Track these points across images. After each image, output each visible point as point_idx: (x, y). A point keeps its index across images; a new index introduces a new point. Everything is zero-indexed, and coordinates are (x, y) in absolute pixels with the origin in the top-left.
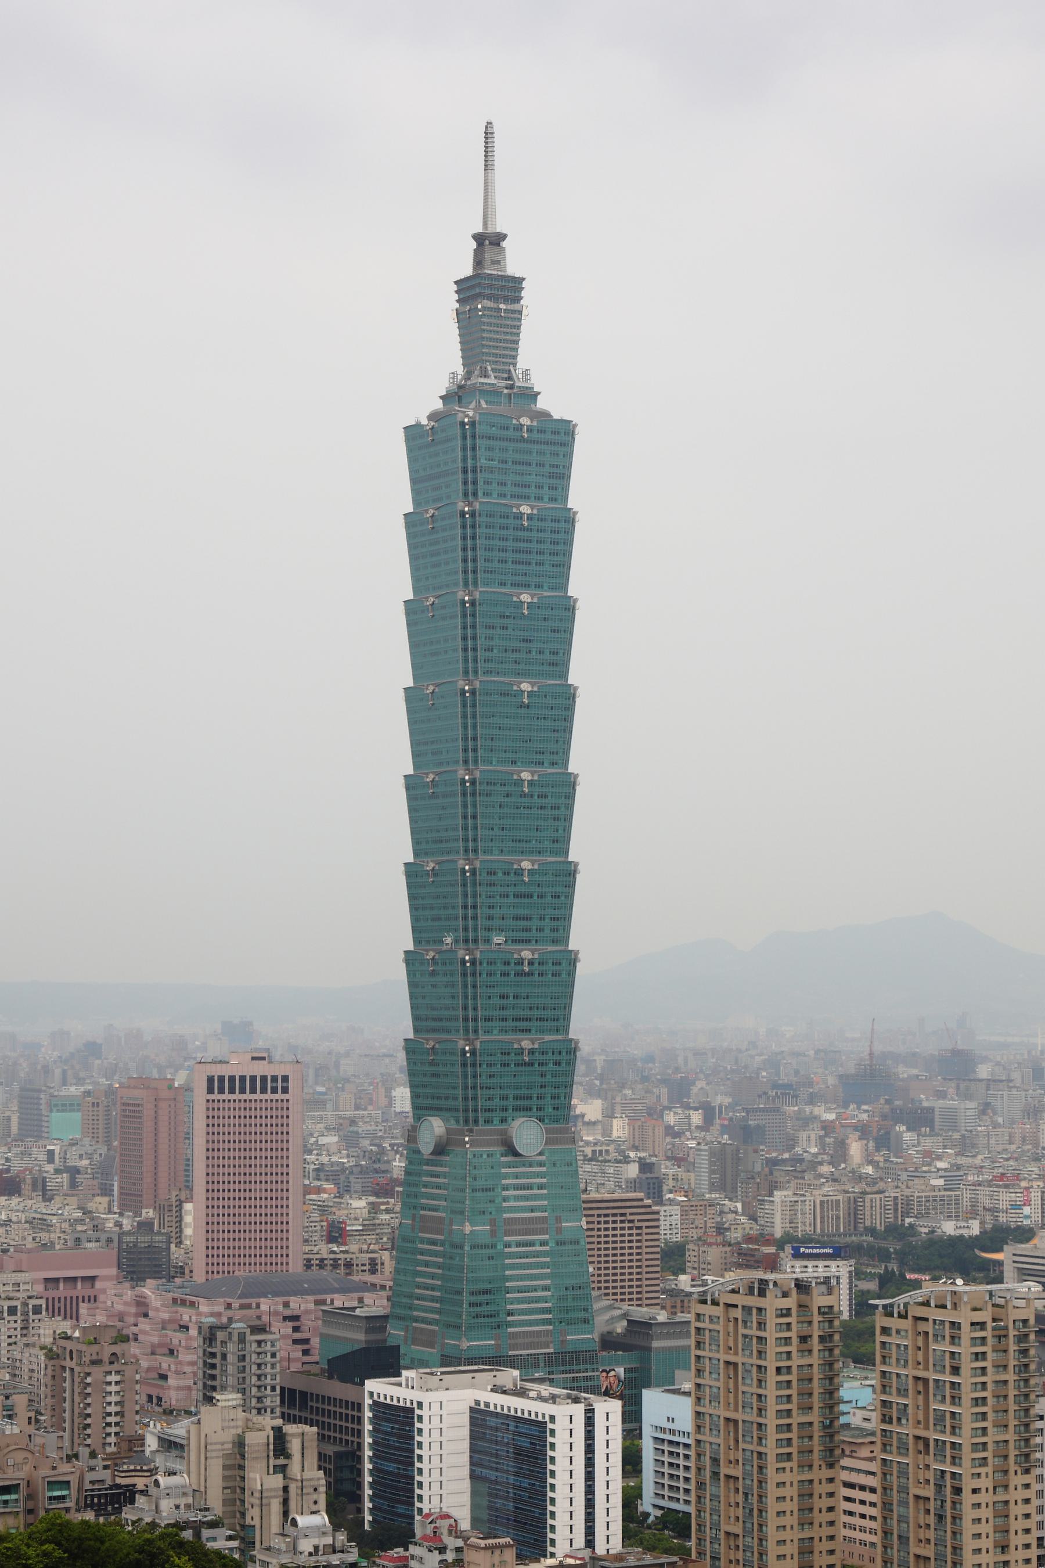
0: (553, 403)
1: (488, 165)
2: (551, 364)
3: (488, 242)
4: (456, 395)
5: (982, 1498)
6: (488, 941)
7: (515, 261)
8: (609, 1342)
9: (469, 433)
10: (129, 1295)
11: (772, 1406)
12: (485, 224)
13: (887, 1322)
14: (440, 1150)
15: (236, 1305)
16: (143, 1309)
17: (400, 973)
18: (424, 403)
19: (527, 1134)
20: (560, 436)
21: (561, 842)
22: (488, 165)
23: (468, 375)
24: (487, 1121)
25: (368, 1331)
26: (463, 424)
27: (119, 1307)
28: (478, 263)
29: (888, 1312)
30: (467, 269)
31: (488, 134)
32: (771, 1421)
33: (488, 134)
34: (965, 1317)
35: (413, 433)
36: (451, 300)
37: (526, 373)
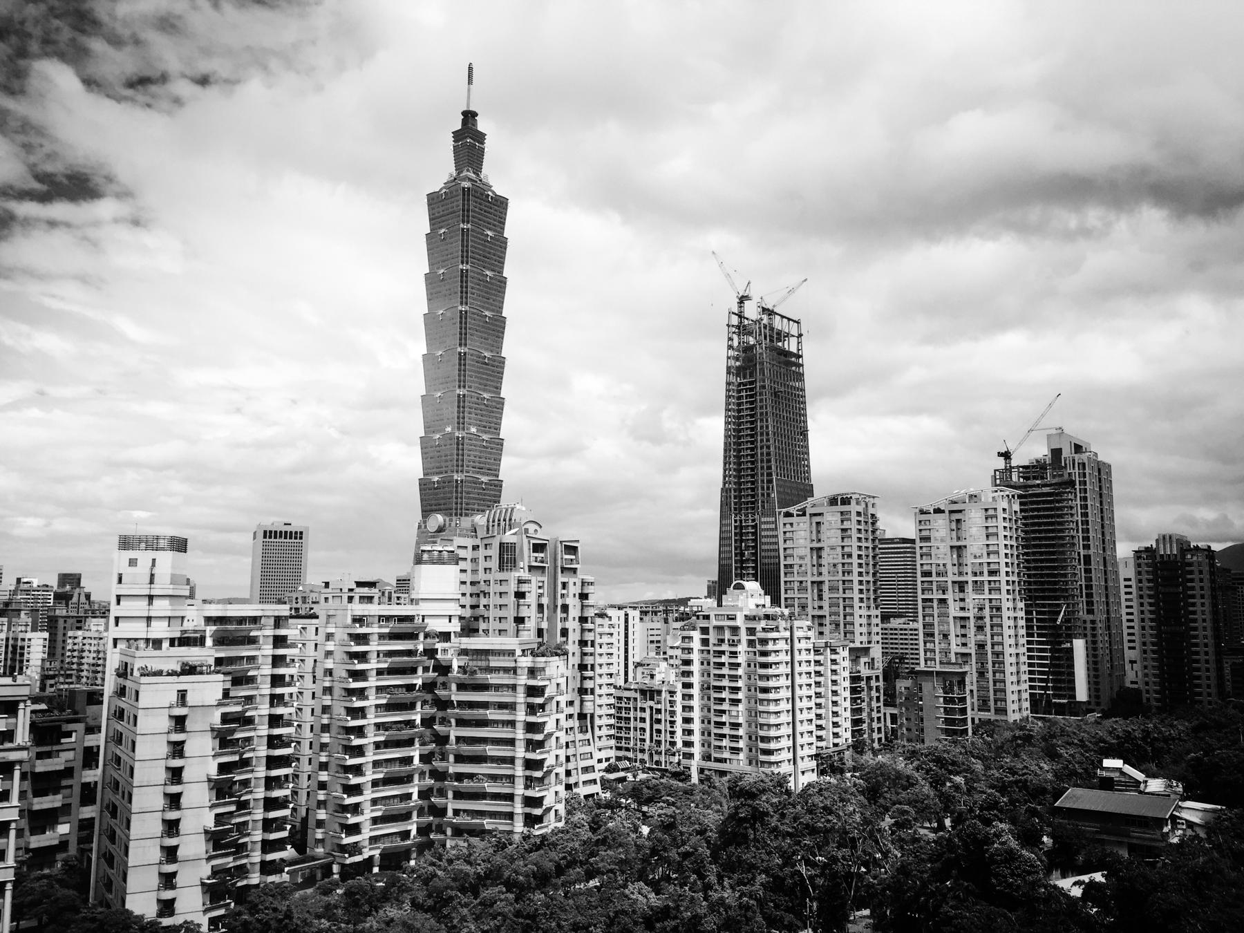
0: (499, 189)
1: (470, 81)
2: (497, 175)
3: (469, 117)
7: (482, 125)
12: (468, 105)
18: (437, 185)
20: (500, 204)
21: (498, 388)
22: (470, 81)
24: (467, 515)
28: (464, 122)
30: (458, 126)
31: (470, 69)
33: (470, 69)
35: (433, 199)
37: (486, 176)
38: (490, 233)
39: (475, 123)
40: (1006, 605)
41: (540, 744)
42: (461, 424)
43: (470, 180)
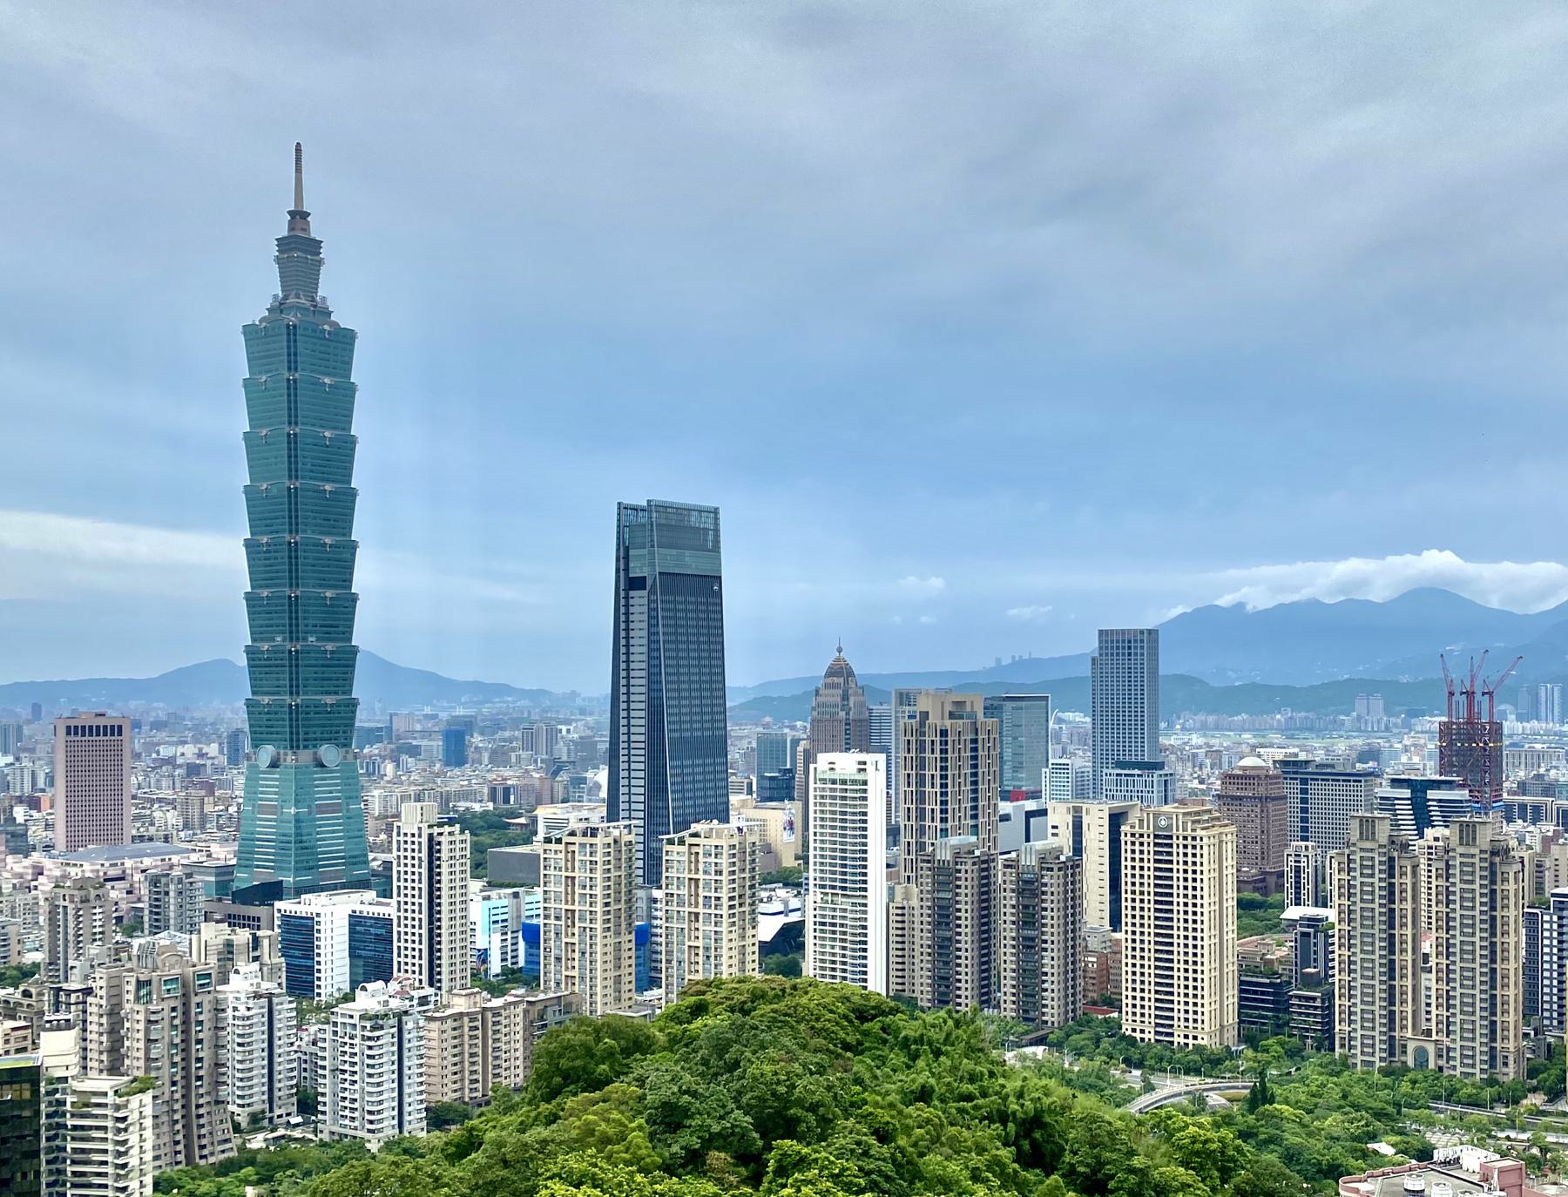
3: (299, 216)
4: (279, 308)
5: (733, 944)
6: (305, 639)
8: (375, 874)
9: (292, 331)
10: (27, 862)
11: (600, 900)
13: (669, 848)
14: (274, 765)
15: (107, 864)
16: (39, 871)
17: (243, 661)
18: (257, 312)
19: (328, 753)
23: (286, 297)
24: (305, 747)
25: (217, 875)
26: (288, 326)
27: (18, 869)
28: (291, 229)
29: (671, 842)
30: (285, 233)
32: (599, 908)
34: (724, 843)
35: (248, 331)
36: (274, 251)
37: (324, 299)
38: (327, 381)
39: (306, 229)
40: (725, 936)
41: (126, 1153)
42: (293, 636)
43: (299, 308)
